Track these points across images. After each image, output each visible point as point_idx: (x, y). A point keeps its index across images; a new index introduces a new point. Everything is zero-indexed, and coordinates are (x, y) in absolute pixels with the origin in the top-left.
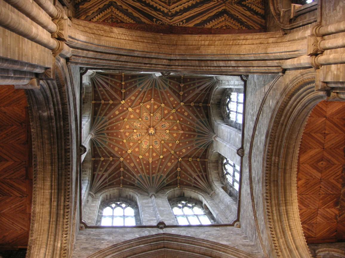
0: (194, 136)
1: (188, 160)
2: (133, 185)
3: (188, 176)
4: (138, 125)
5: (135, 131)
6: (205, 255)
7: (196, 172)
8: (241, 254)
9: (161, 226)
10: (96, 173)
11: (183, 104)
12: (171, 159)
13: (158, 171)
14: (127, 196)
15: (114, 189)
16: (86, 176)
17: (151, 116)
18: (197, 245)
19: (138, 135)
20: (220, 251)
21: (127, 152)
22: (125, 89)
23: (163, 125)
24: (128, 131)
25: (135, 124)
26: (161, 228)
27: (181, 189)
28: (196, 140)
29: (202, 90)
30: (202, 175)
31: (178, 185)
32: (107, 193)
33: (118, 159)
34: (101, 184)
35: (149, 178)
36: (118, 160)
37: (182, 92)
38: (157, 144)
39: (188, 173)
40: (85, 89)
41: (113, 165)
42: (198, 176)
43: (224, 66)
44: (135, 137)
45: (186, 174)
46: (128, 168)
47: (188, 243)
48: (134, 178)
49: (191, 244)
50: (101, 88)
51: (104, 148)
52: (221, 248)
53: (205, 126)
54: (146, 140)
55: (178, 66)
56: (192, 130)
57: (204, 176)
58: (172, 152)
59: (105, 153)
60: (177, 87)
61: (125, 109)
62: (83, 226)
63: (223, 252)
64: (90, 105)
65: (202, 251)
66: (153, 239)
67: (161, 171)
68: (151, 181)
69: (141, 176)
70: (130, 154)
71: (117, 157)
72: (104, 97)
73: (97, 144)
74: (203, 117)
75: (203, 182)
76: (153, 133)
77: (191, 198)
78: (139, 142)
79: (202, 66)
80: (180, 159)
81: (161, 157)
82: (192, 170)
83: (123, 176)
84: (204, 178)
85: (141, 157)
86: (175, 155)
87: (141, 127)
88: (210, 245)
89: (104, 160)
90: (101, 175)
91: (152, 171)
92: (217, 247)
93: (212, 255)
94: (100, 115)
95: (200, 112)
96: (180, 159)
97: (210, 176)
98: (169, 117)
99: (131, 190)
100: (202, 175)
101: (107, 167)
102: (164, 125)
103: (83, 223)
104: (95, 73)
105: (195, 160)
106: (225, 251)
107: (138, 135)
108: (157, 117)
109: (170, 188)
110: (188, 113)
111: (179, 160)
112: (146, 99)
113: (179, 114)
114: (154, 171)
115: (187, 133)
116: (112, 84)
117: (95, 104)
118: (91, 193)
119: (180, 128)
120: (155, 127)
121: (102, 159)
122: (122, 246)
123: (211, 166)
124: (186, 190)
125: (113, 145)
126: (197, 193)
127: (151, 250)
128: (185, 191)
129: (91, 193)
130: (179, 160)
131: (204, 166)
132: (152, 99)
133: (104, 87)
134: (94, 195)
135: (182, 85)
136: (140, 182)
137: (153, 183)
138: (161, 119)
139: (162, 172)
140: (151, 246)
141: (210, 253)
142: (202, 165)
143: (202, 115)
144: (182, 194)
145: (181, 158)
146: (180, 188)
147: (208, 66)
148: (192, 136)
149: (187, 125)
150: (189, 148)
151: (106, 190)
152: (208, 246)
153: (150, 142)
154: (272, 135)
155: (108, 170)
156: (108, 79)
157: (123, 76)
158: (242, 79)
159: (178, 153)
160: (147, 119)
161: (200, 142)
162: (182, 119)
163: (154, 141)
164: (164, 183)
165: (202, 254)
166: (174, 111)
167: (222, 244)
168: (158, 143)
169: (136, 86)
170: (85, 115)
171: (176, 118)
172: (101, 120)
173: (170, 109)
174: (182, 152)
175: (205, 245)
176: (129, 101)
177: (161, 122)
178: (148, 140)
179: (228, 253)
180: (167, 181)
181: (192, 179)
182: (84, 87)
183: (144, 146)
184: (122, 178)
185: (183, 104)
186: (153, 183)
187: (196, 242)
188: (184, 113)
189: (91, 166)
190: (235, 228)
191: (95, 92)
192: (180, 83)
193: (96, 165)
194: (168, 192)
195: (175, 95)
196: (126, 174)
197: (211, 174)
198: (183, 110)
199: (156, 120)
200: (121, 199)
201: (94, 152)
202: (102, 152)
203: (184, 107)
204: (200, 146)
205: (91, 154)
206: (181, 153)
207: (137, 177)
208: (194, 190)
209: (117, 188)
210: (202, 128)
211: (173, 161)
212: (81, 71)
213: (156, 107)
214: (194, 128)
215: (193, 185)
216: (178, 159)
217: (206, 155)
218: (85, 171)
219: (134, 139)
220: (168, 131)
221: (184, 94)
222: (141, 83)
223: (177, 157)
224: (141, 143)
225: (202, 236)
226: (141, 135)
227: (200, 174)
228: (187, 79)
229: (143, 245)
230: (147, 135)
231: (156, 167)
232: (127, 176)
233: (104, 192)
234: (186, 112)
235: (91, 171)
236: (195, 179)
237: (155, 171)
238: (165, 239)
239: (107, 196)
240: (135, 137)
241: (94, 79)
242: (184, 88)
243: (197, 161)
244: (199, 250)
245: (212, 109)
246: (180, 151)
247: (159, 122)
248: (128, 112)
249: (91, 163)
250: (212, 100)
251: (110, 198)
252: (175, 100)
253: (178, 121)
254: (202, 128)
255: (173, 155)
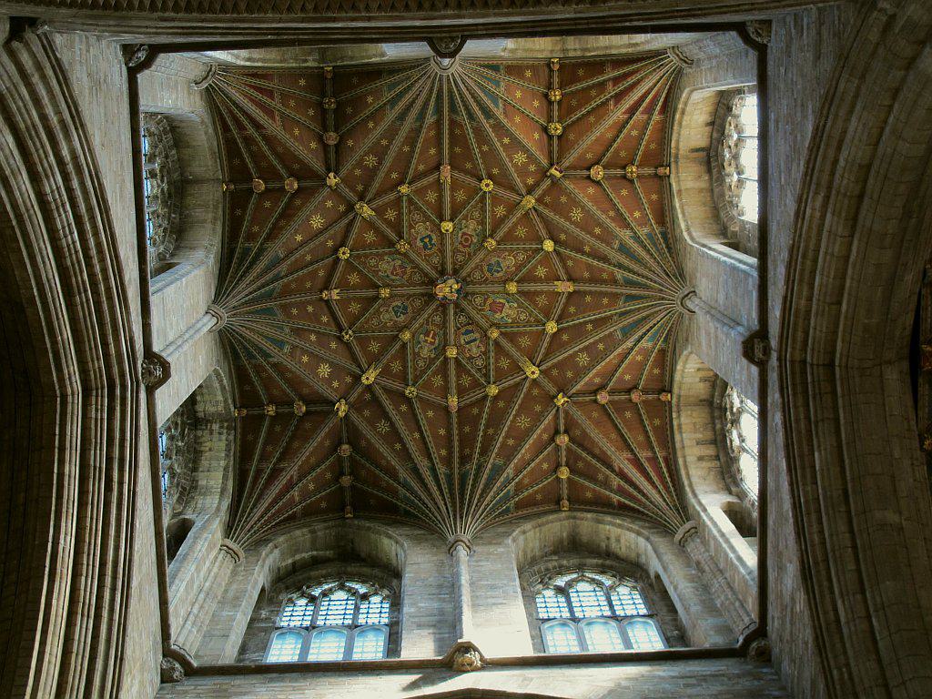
0: (453, 123)
1: (560, 137)
2: (663, 352)
3: (622, 136)
4: (430, 339)
5: (452, 353)
6: (855, 219)
7: (604, 104)
8: (842, 86)
9: (759, 354)
10: (616, 498)
11: (331, 175)
12: (556, 207)
13: (605, 259)
14: (704, 380)
15: (680, 426)
16: (622, 541)
17: (392, 296)
18: (819, 241)
19: (468, 338)
20: (836, 161)
21: (534, 380)
22: (290, 404)
23: (425, 247)
24: (453, 378)
25: (425, 353)
26: (767, 350)
27: (676, 162)
28: (471, 116)
29: (269, 112)
30: (616, 80)
31: (661, 171)
32: (691, 459)
33: (562, 415)
34: (653, 484)
35: (630, 298)
36: (567, 413)
37: (287, 182)
38: (499, 264)
39: (609, 135)
40: (298, 557)
41: (585, 434)
42: (619, 97)
43: (74, 206)
44: (475, 350)
45: (615, 145)
46: (597, 375)
47: (813, 272)
48: (633, 353)
49: (815, 261)
50: (295, 493)
51: (518, 472)
52: (824, 157)
53: (409, 88)
54: (487, 307)
55: (107, 355)
56: (433, 133)
57: (616, 73)
58: (530, 202)
59: (541, 463)
60: (268, 204)
61: (368, 396)
62: (754, 645)
63: (839, 149)
64: (359, 528)
65: (840, 229)
66: (796, 407)
67: (603, 248)
68: (642, 292)
69: (622, 329)
70: (543, 367)
71: (556, 417)
72: (328, 476)
73: (507, 498)
74: (377, 93)
75: (639, 82)
76: (456, 286)
77: (712, 124)
78: (495, 334)
79: (92, 275)
80: (553, 171)
81: (549, 245)
82: (596, 122)
83: (629, 391)
84: (626, 76)
85: (552, 327)
86: (539, 192)
87: (437, 330)
88: (816, 193)
89: (567, 465)
90: (622, 483)
91: (603, 282)
92: (821, 171)
93: (856, 192)
94: (395, 493)
95: (358, 102)
96: (553, 171)
97: (614, 52)
98: (388, 222)
99: (678, 367)
100: (616, 80)
101: (594, 456)
102: (422, 240)
103: (748, 641)
104: (228, 542)
105: (559, 110)
106: (835, 144)
107: (468, 338)
108: (394, 269)
109: (673, 208)
110: (366, 154)
111: (558, 174)
112: (325, 319)
113: (376, 185)
114: (605, 276)
115: (446, 151)
116: (278, 455)
117: (355, 509)
118: (678, 537)
119: (431, 178)
120: (434, 274)
121: (564, 473)
122: (813, 546)
123: (577, 46)
124: (678, 142)
125: (507, 437)
126: (686, 104)
127: (837, 420)
128: (681, 144)
129: (678, 537)
130: (558, 174)
131: (581, 72)
132: (324, 295)
133: (290, 486)
134: (688, 525)
135: (260, 185)
136: (645, 334)
137: (646, 287)
138: (400, 253)
139: (608, 244)
140: (823, 420)
141: (846, 201)
142: (575, 79)
143: (370, 100)
144: (696, 154)
145: (552, 165)
146: (673, 165)
147: (88, 257)
148: (457, 131)
149: (416, 156)
150: (506, 141)
151: (680, 461)
152: (818, 204)
153: (493, 293)
154: (316, 9)
155: (604, 453)
156: (259, 472)
157: (245, 412)
158: (146, 64)
159: (530, 181)
160: (405, 308)
161: (476, 101)
162: (394, 176)
163: (488, 275)
164: (650, 236)
165: (854, 227)
166: (366, 211)
167: (814, 138)
168: (494, 260)
169: (275, 366)
170: (394, 553)
171: (392, 196)
172: (413, 492)
173: (358, 224)
174: (525, 165)
175: (818, 214)
176: (336, 384)
177: (413, 256)
178: (486, 300)
179: (845, 132)
180: (643, 222)
181: (632, 122)
182: (290, 561)
183: (509, 312)
184: (635, 396)
185: (331, 175)
186: (646, 287)
187: (807, 242)
188: (366, 168)
189: (589, 515)
190: (775, 46)
191: (310, 512)
192: (251, 191)
193: (589, 495)
194: (683, 226)
195: (299, 208)
196: (621, 379)
197: (606, 48)
198: (358, 172)
199: (404, 273)
200: (717, 401)
201: (535, 504)
202: (537, 476)
203: (344, 172)
204: (495, 98)
205: (544, 519)
206: (532, 168)
207: (629, 344)
208: (677, 116)
209: (674, 415)
210: (419, 103)
211: (563, 199)
212: (176, 675)
213: (354, 279)
214: (424, 130)
215: (656, 117)
216: (555, 182)
217: (534, 68)
218: (608, 539)
219: (485, 353)
220: (447, 226)
221: (292, 174)
222: (260, 350)
223: (548, 182)
224: (497, 326)
225: (791, 205)
226: (470, 328)
227: (612, 90)
228: (231, 168)
229: (816, 454)
230: (464, 304)
231: (589, 267)
232: (627, 377)
233: (683, 472)
234: (362, 160)
235: (608, 518)
236: (632, 111)
237: (604, 271)
238: (798, 357)
239: (701, 459)
240: (475, 350)
241: (243, 544)
242: (269, 174)
243: (560, 102)
244: (839, 239)
245: (342, 59)
246: (523, 171)
247: (412, 261)
248: (378, 384)
249: (578, 514)
250: (306, 61)
251: (714, 442)
252: (321, 209)
253: (404, 189)
254: (419, 103)
255: (539, 200)
